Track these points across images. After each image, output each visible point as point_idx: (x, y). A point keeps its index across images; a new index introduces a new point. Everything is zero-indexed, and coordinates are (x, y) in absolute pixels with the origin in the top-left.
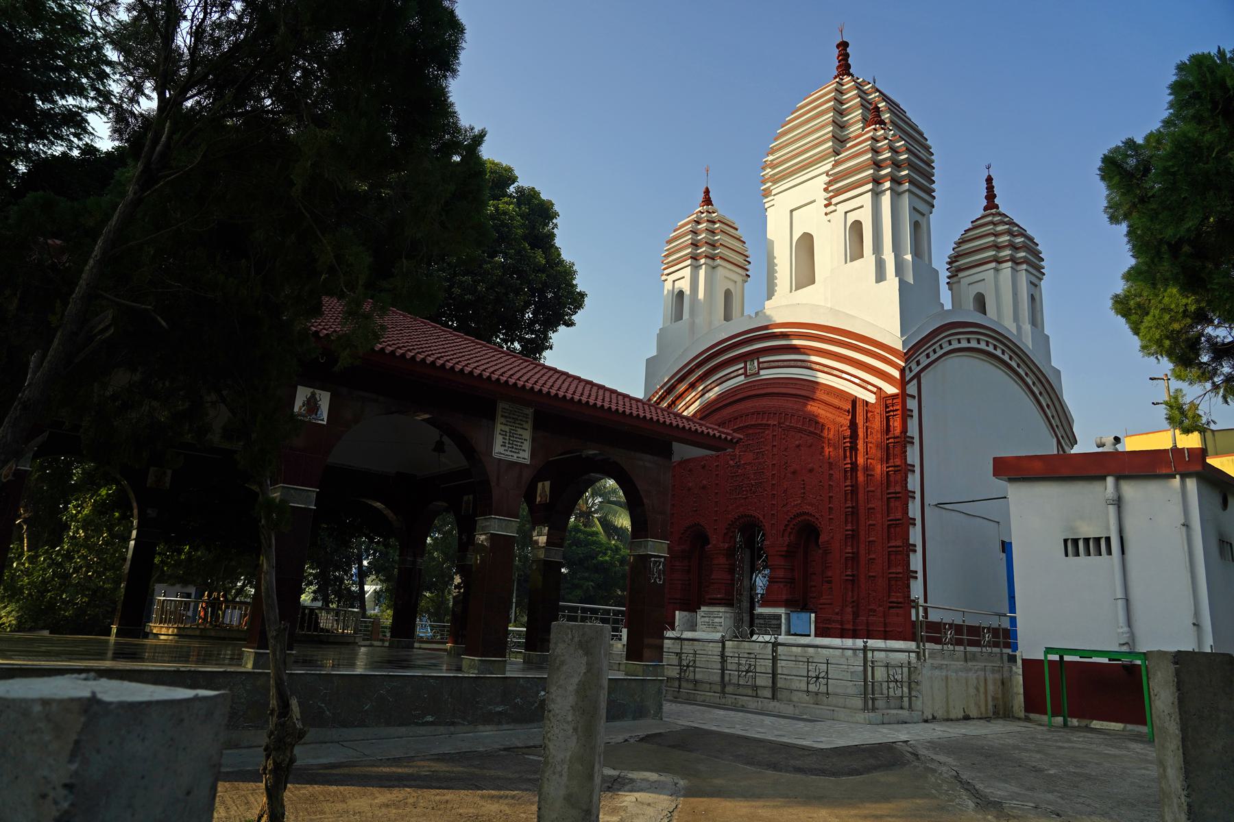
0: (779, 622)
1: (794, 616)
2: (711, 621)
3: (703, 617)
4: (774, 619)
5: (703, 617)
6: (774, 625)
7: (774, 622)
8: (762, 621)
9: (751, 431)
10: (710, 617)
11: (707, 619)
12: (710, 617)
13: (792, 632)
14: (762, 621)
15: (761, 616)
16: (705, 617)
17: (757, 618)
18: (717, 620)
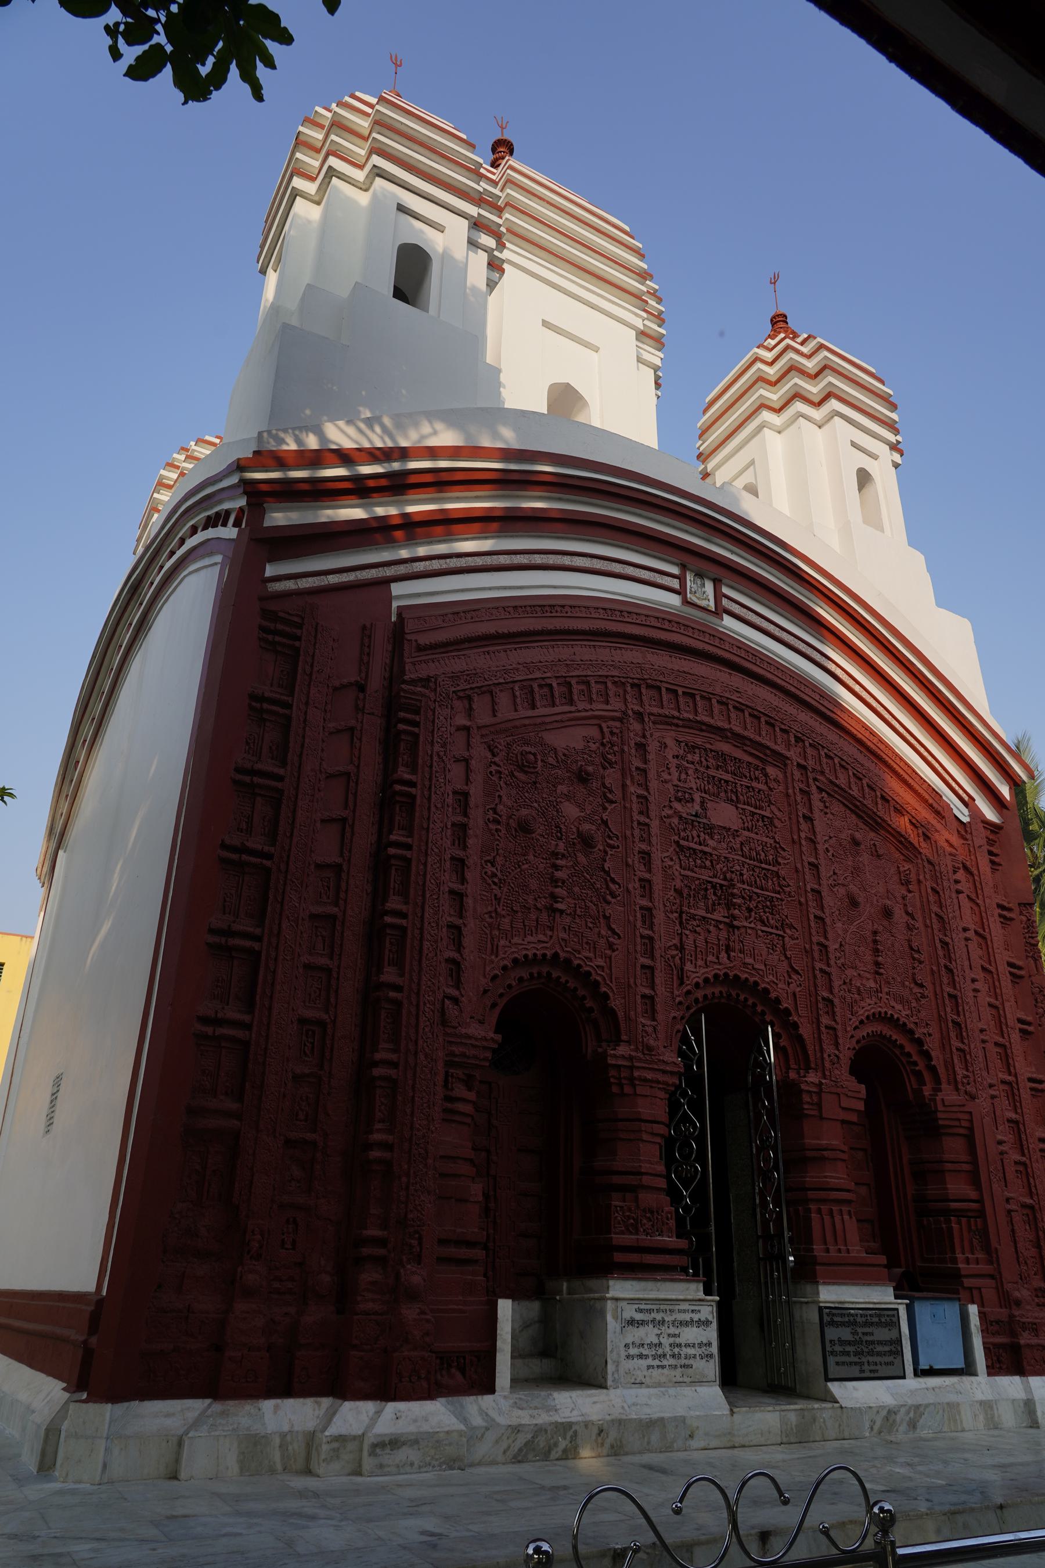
0: (893, 1335)
1: (924, 1310)
2: (666, 1341)
3: (632, 1322)
4: (879, 1324)
5: (632, 1322)
6: (880, 1343)
7: (882, 1334)
8: (845, 1334)
9: (725, 747)
10: (662, 1322)
11: (649, 1334)
12: (662, 1322)
13: (924, 1365)
14: (845, 1334)
15: (834, 1315)
16: (642, 1323)
17: (832, 1323)
18: (690, 1335)
